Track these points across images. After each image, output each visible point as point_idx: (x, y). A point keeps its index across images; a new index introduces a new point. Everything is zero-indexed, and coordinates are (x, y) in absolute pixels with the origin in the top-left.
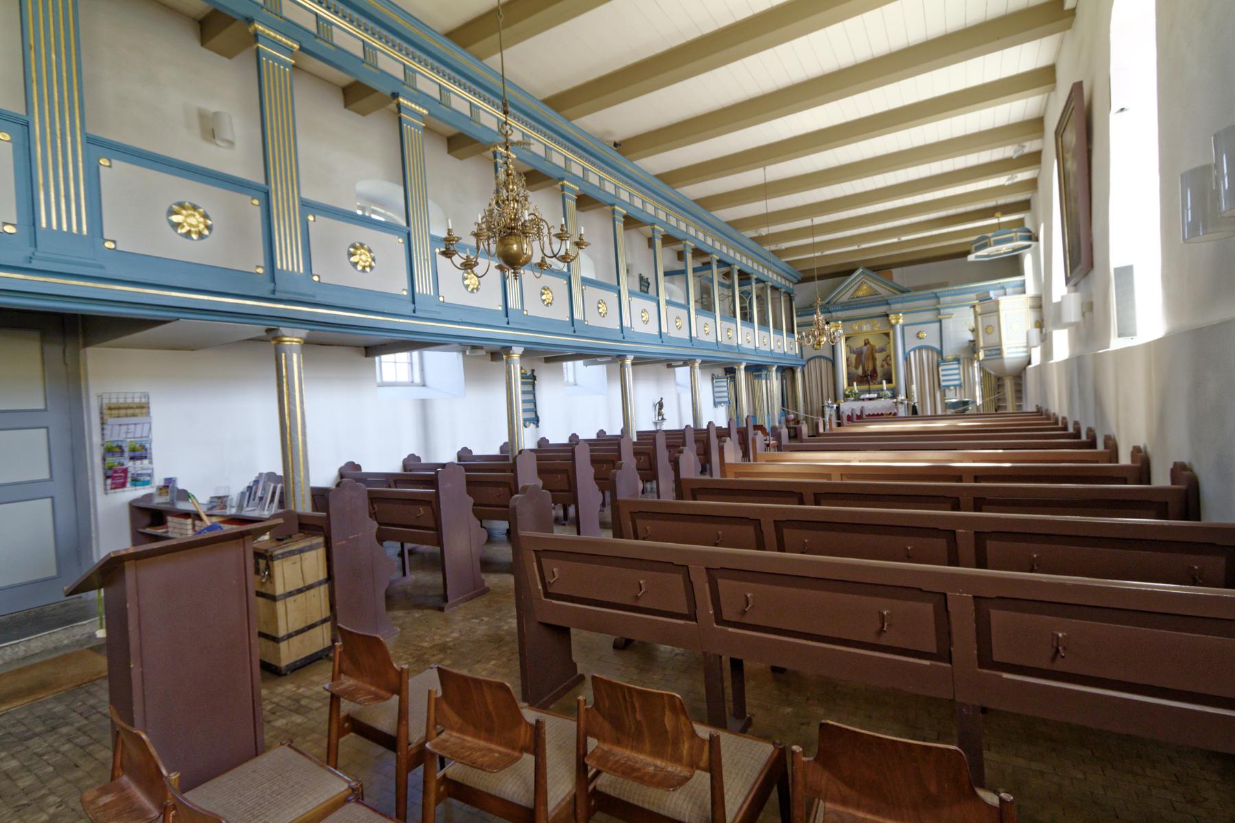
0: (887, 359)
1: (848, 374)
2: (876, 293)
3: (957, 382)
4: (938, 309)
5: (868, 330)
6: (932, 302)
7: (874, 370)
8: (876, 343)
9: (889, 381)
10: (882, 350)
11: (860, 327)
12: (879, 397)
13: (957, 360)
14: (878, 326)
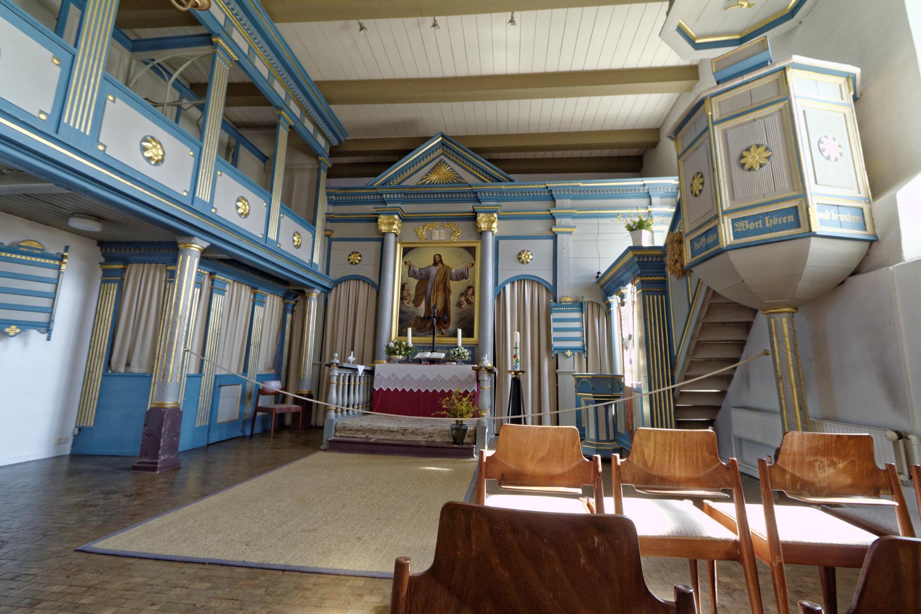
1: (401, 312)
2: (460, 182)
3: (578, 344)
5: (442, 240)
6: (540, 206)
7: (446, 310)
8: (454, 263)
9: (468, 333)
10: (462, 276)
11: (430, 234)
12: (448, 360)
13: (580, 306)
14: (460, 235)
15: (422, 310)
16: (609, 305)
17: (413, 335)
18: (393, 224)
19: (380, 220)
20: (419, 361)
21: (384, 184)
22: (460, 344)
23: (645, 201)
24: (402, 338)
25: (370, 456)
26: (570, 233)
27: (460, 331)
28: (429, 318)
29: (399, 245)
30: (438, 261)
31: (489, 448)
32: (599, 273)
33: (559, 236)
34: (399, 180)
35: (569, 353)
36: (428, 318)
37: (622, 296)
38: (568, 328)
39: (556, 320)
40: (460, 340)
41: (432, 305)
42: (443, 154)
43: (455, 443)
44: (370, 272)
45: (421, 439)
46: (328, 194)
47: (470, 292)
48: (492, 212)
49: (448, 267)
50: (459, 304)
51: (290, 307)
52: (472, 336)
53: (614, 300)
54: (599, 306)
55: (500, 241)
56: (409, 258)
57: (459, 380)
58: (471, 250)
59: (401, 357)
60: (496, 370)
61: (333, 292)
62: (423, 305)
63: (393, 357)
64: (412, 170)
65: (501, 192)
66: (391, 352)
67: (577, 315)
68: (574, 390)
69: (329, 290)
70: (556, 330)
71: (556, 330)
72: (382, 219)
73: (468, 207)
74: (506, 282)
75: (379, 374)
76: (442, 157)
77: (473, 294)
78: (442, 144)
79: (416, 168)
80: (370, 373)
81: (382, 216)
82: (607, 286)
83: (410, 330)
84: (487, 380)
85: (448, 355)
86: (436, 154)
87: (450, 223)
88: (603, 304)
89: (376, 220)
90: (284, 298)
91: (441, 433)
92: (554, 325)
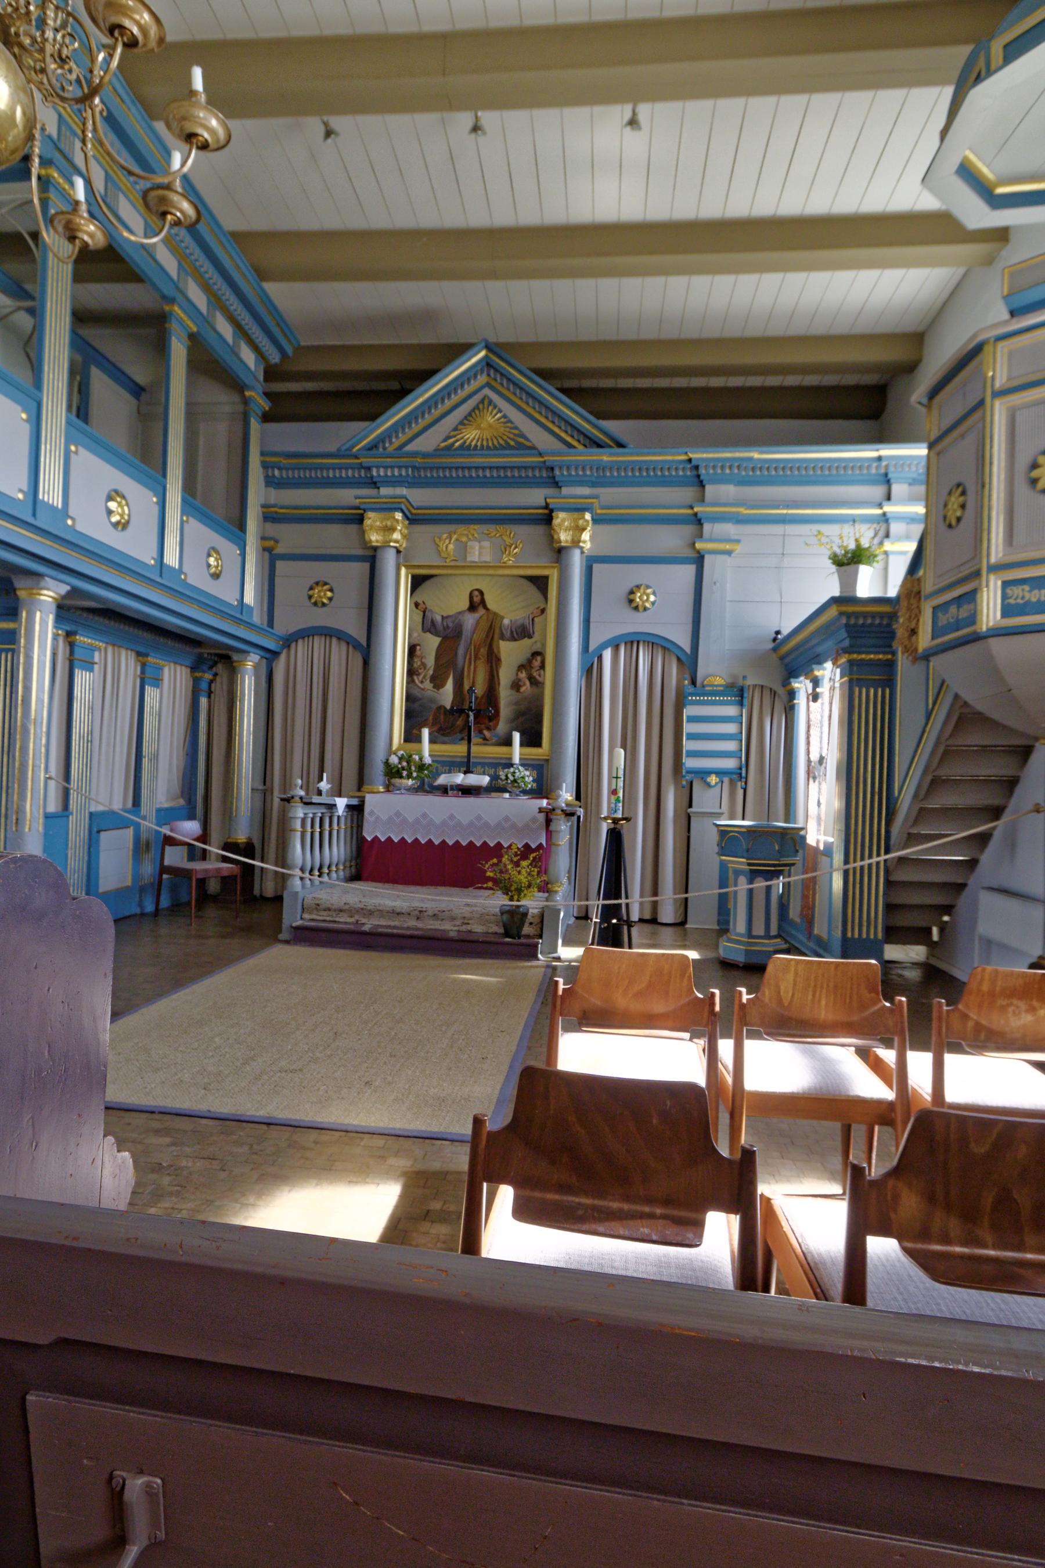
1: (410, 698)
2: (523, 446)
3: (730, 764)
4: (698, 521)
5: (484, 560)
6: (675, 497)
7: (492, 695)
8: (508, 606)
9: (532, 739)
10: (522, 632)
12: (495, 788)
13: (738, 693)
14: (521, 552)
15: (447, 695)
16: (792, 694)
17: (432, 741)
18: (393, 529)
19: (367, 522)
20: (444, 790)
21: (373, 447)
22: (516, 760)
23: (879, 491)
25: (364, 953)
26: (729, 553)
27: (517, 737)
28: (461, 711)
29: (403, 571)
30: (477, 602)
31: (567, 943)
32: (778, 633)
33: (708, 559)
34: (403, 438)
35: (713, 779)
36: (458, 710)
37: (816, 682)
38: (714, 733)
39: (692, 719)
40: (517, 751)
41: (466, 687)
42: (488, 385)
43: (507, 934)
45: (449, 928)
46: (265, 466)
47: (537, 663)
48: (582, 510)
49: (495, 614)
50: (516, 686)
51: (204, 686)
52: (538, 744)
53: (802, 686)
54: (774, 693)
55: (595, 566)
56: (423, 594)
57: (514, 826)
58: (540, 583)
59: (410, 782)
60: (581, 812)
61: (283, 657)
63: (397, 781)
64: (428, 419)
65: (601, 467)
66: (392, 773)
67: (731, 711)
68: (716, 849)
69: (275, 654)
70: (692, 737)
71: (692, 737)
72: (372, 519)
73: (535, 497)
74: (604, 646)
75: (372, 813)
76: (487, 391)
77: (542, 666)
78: (487, 364)
79: (436, 413)
80: (357, 810)
81: (371, 515)
82: (789, 660)
83: (426, 733)
84: (564, 829)
85: (495, 778)
86: (474, 385)
87: (501, 528)
88: (781, 691)
89: (360, 520)
90: (193, 669)
91: (482, 918)
92: (688, 728)
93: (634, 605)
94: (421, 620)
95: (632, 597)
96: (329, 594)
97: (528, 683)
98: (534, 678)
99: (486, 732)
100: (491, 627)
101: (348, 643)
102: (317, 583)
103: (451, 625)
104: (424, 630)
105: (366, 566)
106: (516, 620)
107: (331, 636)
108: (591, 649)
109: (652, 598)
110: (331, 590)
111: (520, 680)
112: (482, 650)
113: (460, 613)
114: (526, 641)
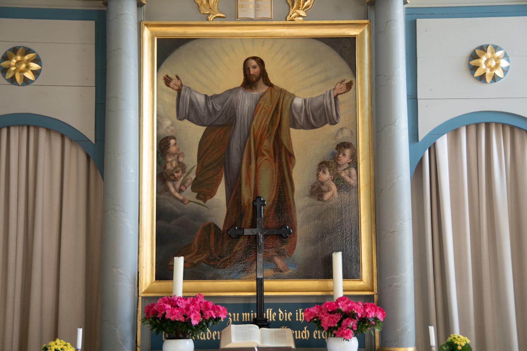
0: (338, 158)
1: (162, 214)
8: (298, 81)
10: (320, 116)
24: (163, 284)
29: (147, 33)
30: (255, 75)
36: (232, 231)
41: (247, 196)
44: (74, 109)
49: (281, 90)
50: (317, 191)
55: (419, 21)
56: (176, 66)
58: (345, 47)
62: (221, 195)
74: (438, 132)
77: (354, 163)
93: (478, 73)
94: (175, 103)
95: (474, 62)
96: (35, 66)
97: (334, 187)
98: (344, 181)
99: (277, 260)
100: (277, 110)
101: (63, 136)
102: (15, 51)
103: (218, 108)
104: (180, 117)
105: (90, 26)
106: (312, 99)
107: (37, 127)
108: (421, 137)
109: (504, 63)
110: (37, 60)
111: (322, 183)
112: (266, 143)
113: (231, 91)
114: (328, 129)
